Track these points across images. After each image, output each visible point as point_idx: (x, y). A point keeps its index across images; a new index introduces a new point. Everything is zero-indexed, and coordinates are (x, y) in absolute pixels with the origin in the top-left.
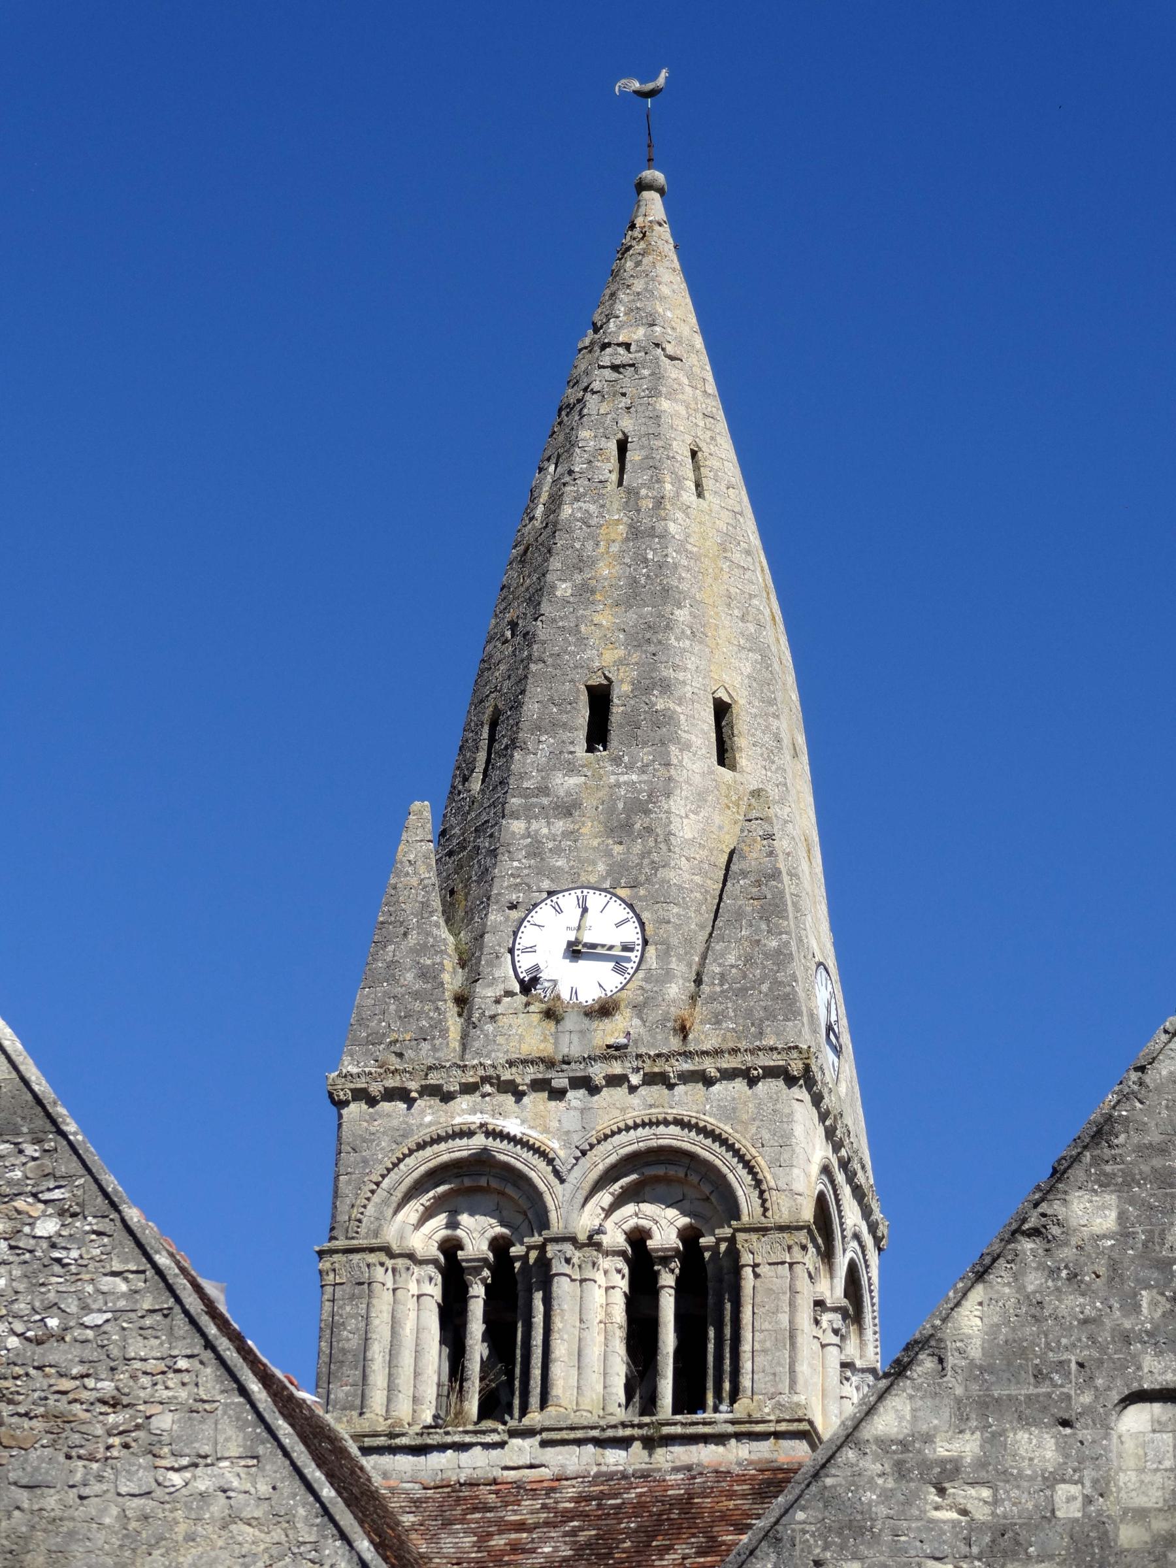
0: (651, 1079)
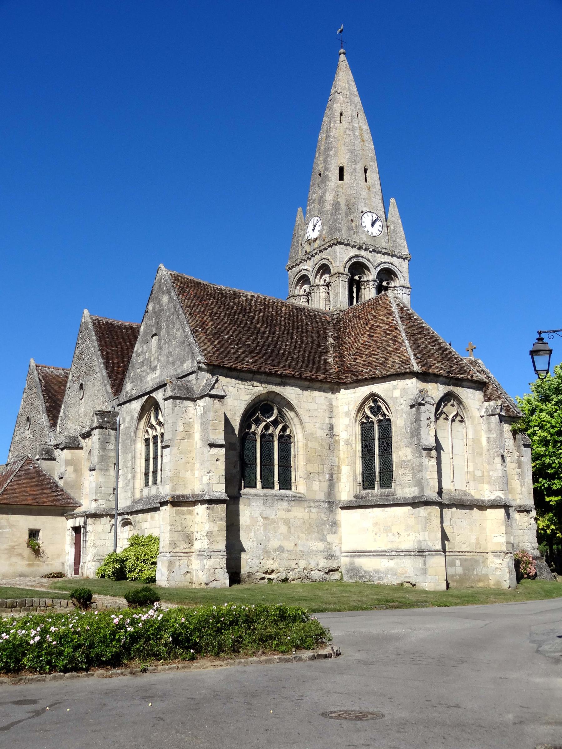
0: (320, 251)
